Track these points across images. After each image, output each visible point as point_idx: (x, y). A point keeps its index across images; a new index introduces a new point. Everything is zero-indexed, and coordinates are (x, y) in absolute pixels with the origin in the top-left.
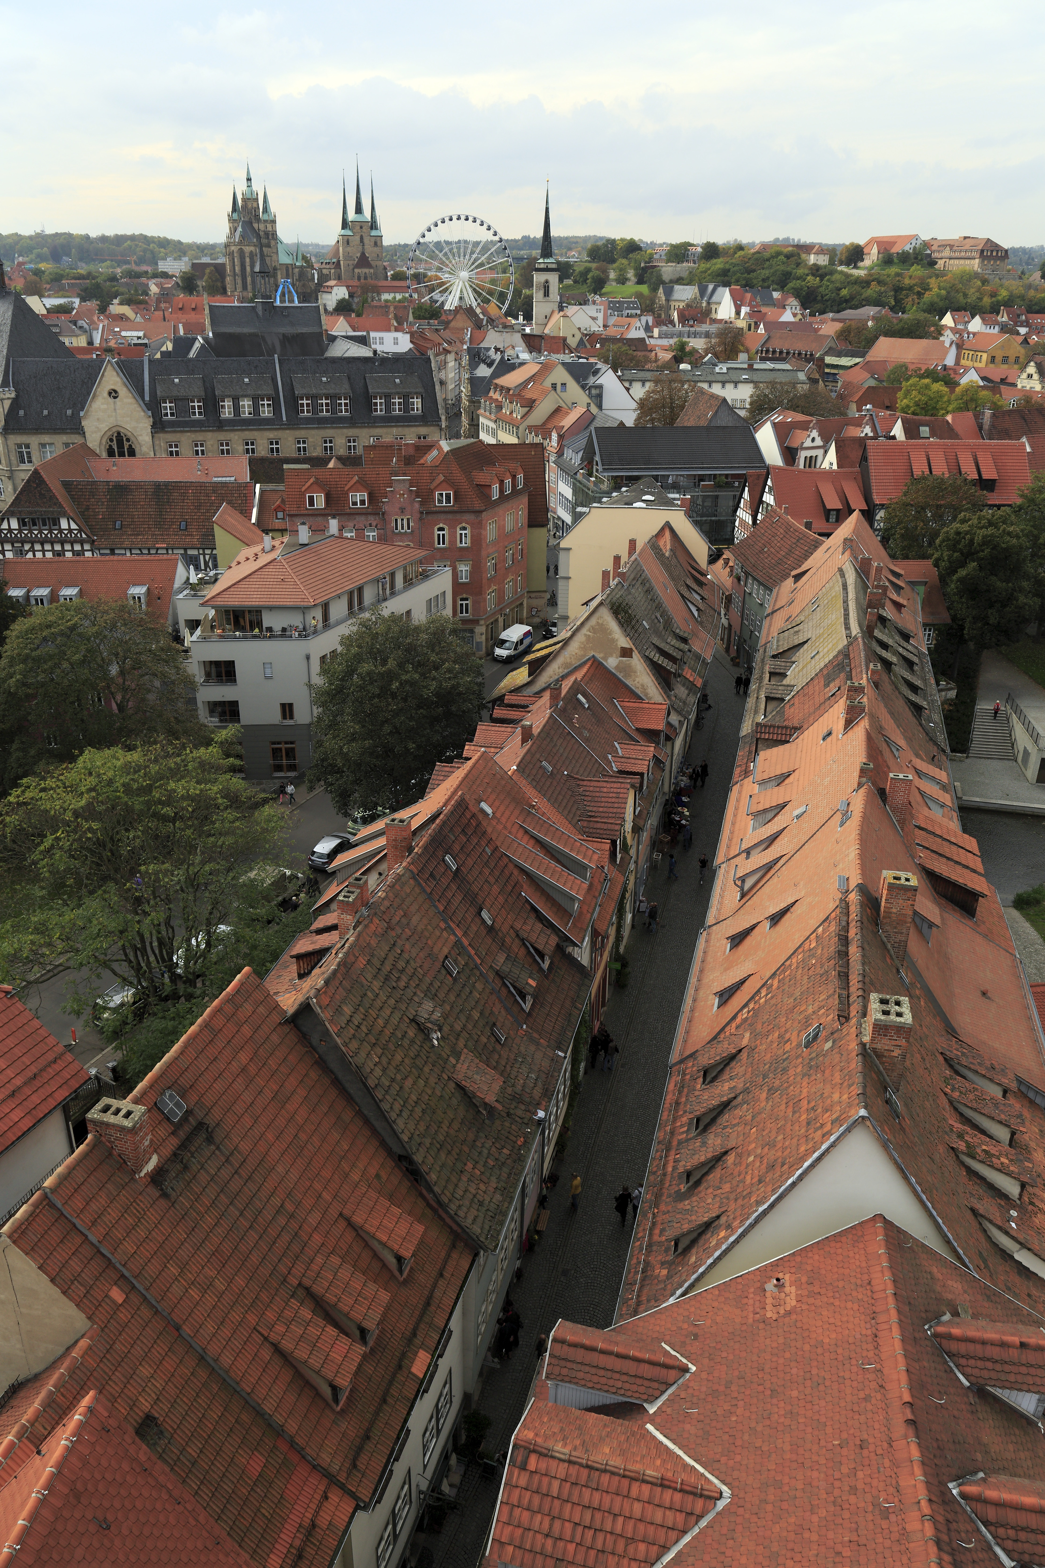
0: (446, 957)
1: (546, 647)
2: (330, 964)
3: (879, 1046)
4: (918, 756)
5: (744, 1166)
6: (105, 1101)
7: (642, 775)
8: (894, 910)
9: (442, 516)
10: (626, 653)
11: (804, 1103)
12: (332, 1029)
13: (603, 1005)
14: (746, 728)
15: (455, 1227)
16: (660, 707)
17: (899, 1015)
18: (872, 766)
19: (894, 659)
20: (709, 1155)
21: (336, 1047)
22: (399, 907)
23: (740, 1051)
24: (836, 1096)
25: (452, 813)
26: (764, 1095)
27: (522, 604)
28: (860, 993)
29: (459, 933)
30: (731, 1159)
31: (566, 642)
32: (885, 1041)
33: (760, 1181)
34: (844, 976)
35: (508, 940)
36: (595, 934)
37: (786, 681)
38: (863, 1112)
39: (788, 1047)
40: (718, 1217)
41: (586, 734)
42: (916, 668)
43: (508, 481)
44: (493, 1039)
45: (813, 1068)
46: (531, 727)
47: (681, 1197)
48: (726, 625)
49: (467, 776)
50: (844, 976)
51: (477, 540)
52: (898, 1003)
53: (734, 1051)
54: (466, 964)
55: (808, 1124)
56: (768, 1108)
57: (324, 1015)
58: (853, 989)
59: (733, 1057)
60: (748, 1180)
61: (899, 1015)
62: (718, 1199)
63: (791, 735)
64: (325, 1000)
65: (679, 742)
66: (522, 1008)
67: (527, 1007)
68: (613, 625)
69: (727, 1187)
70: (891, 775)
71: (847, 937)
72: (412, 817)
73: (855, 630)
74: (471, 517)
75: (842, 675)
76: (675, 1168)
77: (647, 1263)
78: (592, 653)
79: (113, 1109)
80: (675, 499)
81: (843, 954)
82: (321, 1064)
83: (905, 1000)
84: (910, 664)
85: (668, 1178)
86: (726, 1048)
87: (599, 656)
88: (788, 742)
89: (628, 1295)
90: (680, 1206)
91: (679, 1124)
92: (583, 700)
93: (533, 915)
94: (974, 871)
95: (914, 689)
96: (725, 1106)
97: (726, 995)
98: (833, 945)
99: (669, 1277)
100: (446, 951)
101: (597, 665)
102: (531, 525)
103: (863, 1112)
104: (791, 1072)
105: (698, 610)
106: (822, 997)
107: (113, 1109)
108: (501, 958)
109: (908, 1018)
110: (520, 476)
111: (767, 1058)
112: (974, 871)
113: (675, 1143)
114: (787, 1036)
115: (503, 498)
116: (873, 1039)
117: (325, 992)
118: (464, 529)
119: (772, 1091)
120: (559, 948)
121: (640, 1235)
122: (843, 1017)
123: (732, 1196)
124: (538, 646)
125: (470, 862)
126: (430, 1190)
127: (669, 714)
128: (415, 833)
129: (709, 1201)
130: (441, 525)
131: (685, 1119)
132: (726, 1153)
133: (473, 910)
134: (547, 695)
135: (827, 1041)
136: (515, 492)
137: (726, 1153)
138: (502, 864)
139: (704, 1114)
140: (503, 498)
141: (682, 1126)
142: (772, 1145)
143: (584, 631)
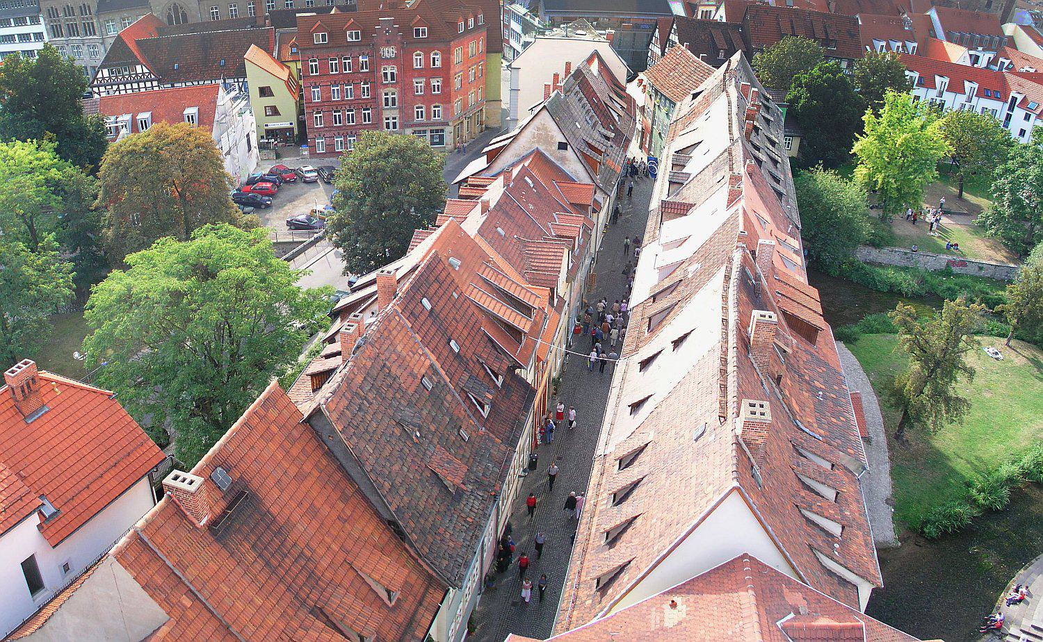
0: (424, 376)
1: (501, 141)
2: (337, 378)
3: (747, 437)
4: (779, 228)
5: (649, 525)
6: (175, 472)
7: (574, 238)
8: (760, 339)
9: (419, 46)
10: (562, 146)
11: (693, 480)
12: (338, 428)
13: (544, 414)
14: (654, 204)
15: (430, 571)
16: (589, 187)
17: (762, 414)
18: (746, 233)
19: (763, 157)
20: (623, 520)
21: (341, 441)
22: (387, 338)
23: (647, 445)
24: (717, 475)
25: (428, 267)
26: (664, 476)
27: (482, 110)
28: (735, 399)
29: (433, 358)
30: (639, 521)
31: (515, 137)
32: (752, 433)
33: (660, 536)
34: (724, 388)
35: (471, 365)
36: (539, 359)
37: (684, 171)
38: (736, 484)
39: (682, 441)
40: (630, 562)
41: (531, 207)
42: (778, 165)
43: (471, 22)
44: (459, 438)
45: (700, 454)
46: (488, 202)
47: (599, 550)
48: (640, 129)
49: (438, 239)
50: (724, 388)
51: (447, 62)
52: (762, 406)
53: (642, 445)
54: (439, 382)
55: (696, 494)
56: (667, 484)
57: (333, 417)
58: (730, 397)
59: (641, 450)
60: (652, 535)
61: (762, 414)
62: (629, 550)
63: (688, 211)
64: (333, 407)
65: (603, 214)
66: (482, 416)
67: (485, 414)
68: (552, 126)
69: (636, 541)
70: (760, 241)
71: (726, 360)
72: (397, 270)
73: (736, 135)
74: (442, 46)
75: (727, 168)
76: (597, 530)
77: (576, 597)
78: (536, 146)
79: (180, 479)
80: (601, 34)
81: (724, 372)
82: (330, 454)
83: (767, 404)
84: (775, 162)
85: (592, 536)
86: (636, 443)
87: (542, 148)
88: (686, 215)
89: (561, 617)
90: (601, 555)
91: (600, 498)
92: (530, 182)
93: (490, 345)
94: (815, 312)
95: (778, 181)
96: (636, 485)
97: (636, 407)
98: (717, 364)
99: (593, 605)
100: (423, 371)
101: (539, 156)
102: (488, 52)
103: (736, 484)
104: (684, 458)
105: (619, 115)
106: (708, 404)
107: (180, 479)
108: (466, 377)
109: (768, 417)
110: (481, 16)
111: (667, 450)
112: (815, 312)
113: (597, 512)
114: (682, 433)
115: (467, 31)
116: (744, 432)
117: (332, 400)
118: (436, 54)
119: (669, 473)
120: (511, 370)
121: (571, 577)
122: (723, 417)
123: (639, 547)
124: (494, 140)
125: (441, 304)
126: (412, 545)
127: (595, 192)
128: (399, 281)
129: (623, 551)
130: (418, 52)
131: (605, 495)
132: (636, 517)
133: (444, 341)
134: (501, 178)
135: (710, 435)
136: (476, 26)
137: (636, 517)
138: (466, 305)
139: (619, 490)
140: (467, 31)
141: (602, 500)
142: (669, 510)
143: (530, 130)
